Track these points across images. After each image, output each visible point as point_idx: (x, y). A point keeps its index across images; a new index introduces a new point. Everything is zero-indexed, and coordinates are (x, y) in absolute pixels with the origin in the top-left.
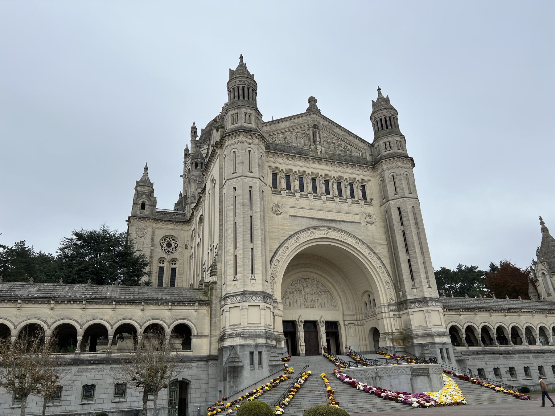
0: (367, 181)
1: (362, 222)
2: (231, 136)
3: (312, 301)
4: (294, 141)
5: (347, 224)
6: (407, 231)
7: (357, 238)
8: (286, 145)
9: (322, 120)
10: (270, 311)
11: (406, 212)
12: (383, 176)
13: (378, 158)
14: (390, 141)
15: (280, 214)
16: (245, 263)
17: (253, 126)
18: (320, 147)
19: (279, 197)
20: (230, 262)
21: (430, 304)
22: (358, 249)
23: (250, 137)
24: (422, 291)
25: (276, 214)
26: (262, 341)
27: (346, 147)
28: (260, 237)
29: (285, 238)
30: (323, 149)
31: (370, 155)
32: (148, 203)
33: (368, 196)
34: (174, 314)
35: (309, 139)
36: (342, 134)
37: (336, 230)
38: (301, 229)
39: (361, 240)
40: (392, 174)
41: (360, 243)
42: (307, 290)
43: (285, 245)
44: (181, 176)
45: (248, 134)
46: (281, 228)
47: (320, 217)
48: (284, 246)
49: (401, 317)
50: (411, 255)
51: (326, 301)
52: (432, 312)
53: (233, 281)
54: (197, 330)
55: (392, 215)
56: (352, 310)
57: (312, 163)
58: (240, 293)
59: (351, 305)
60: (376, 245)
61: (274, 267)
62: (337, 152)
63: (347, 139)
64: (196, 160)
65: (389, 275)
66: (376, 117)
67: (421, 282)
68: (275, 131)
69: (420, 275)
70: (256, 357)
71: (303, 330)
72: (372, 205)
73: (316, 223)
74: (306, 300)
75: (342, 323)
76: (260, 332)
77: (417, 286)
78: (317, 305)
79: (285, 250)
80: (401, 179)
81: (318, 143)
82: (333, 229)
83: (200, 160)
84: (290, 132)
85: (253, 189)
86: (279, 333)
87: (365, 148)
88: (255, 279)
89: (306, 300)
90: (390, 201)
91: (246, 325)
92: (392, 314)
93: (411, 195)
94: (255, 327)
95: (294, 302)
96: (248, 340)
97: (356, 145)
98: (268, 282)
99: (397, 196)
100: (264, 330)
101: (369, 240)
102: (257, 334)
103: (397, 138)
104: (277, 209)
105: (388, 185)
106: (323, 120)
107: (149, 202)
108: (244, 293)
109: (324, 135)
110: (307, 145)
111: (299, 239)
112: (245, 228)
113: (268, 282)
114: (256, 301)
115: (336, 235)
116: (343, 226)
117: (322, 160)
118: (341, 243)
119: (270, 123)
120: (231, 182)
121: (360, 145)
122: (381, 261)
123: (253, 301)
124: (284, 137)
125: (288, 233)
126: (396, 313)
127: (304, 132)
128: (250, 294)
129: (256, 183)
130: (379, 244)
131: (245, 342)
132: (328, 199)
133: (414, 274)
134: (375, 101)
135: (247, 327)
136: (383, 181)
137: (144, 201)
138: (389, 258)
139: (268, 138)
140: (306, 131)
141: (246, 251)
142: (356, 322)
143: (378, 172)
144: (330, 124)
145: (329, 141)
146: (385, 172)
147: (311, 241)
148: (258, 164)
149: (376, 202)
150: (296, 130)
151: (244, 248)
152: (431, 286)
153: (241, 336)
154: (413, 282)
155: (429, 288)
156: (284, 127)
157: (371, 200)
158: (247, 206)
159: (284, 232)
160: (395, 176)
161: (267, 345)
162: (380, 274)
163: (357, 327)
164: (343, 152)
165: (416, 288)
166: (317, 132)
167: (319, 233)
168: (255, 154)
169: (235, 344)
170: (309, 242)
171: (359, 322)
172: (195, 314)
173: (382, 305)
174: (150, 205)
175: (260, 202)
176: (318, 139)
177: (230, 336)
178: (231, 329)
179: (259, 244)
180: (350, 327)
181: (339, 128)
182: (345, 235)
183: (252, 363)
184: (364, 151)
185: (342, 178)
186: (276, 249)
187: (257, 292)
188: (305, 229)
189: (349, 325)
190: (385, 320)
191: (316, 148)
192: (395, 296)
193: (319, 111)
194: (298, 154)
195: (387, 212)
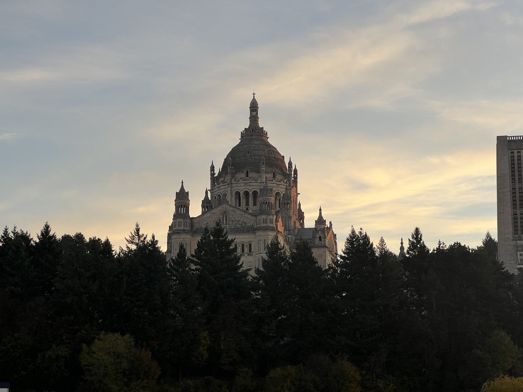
0: (252, 242)
17: (182, 228)
23: (179, 235)
30: (228, 226)
36: (241, 214)
45: (178, 234)
63: (244, 217)
72: (252, 256)
80: (261, 243)
83: (205, 204)
99: (259, 252)
127: (218, 217)
140: (220, 216)
150: (214, 217)
157: (253, 252)
164: (240, 225)
176: (225, 221)
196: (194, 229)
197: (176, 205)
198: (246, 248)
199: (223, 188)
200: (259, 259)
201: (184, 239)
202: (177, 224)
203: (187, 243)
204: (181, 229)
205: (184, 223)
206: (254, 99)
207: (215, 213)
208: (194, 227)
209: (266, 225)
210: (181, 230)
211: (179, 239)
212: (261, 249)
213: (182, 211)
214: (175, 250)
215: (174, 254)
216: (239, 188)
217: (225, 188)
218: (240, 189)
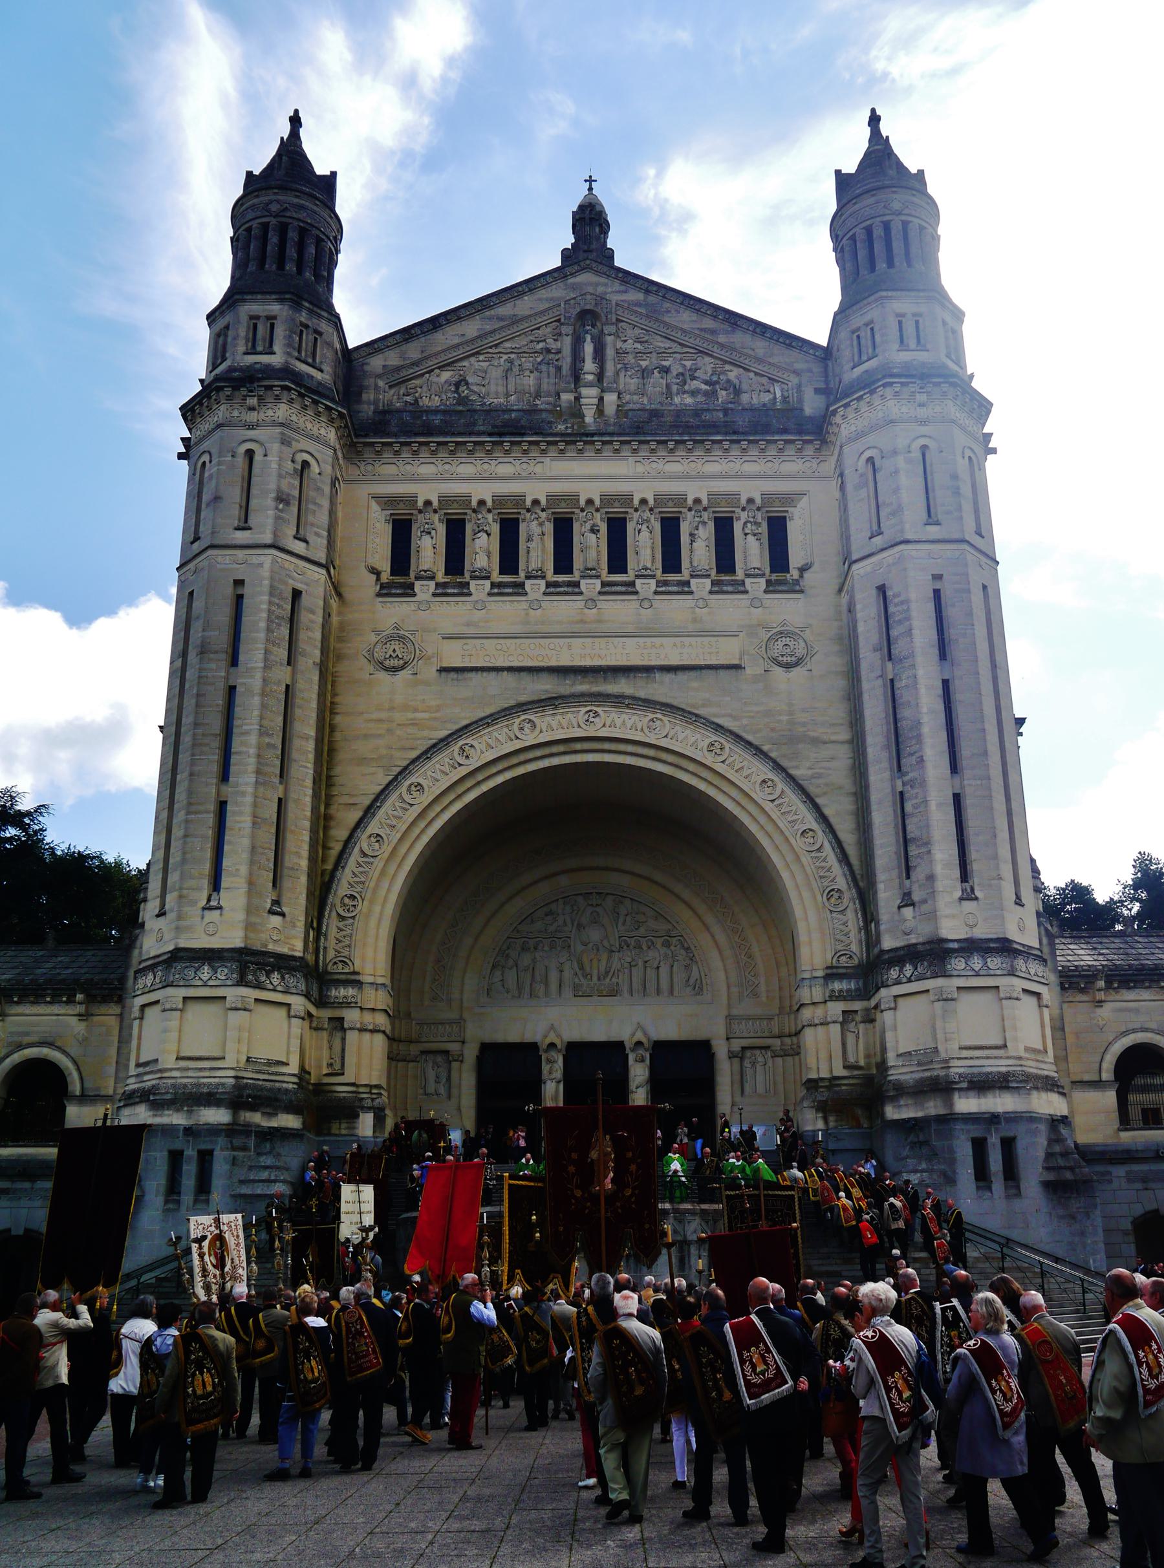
0: (790, 499)
1: (746, 662)
3: (607, 973)
4: (493, 388)
5: (682, 677)
6: (901, 680)
7: (718, 728)
8: (460, 408)
9: (617, 286)
10: (289, 1016)
11: (902, 603)
14: (872, 322)
15: (403, 668)
16: (188, 856)
18: (594, 391)
19: (405, 605)
21: (957, 964)
22: (719, 768)
23: (253, 401)
24: (933, 916)
25: (387, 669)
26: (217, 1116)
27: (715, 378)
28: (252, 760)
29: (414, 754)
31: (817, 391)
33: (795, 559)
34: (13, 1030)
35: (559, 369)
36: (701, 330)
37: (628, 706)
38: (482, 715)
39: (731, 733)
40: (867, 454)
41: (727, 746)
42: (595, 935)
43: (413, 779)
46: (398, 717)
47: (565, 661)
48: (407, 783)
49: (872, 1021)
50: (907, 773)
51: (664, 971)
52: (967, 999)
53: (158, 916)
54: (81, 1079)
56: (764, 999)
57: (554, 458)
58: (165, 957)
59: (762, 980)
60: (800, 746)
61: (360, 860)
62: (677, 400)
63: (722, 346)
65: (844, 858)
67: (931, 878)
68: (416, 364)
69: (929, 852)
70: (190, 1170)
71: (558, 1073)
72: (802, 592)
73: (546, 686)
74: (582, 968)
75: (721, 1050)
76: (218, 1085)
77: (916, 897)
78: (625, 988)
79: (407, 798)
80: (896, 472)
81: (590, 377)
84: (481, 358)
85: (247, 591)
86: (362, 1090)
87: (799, 366)
88: (220, 908)
89: (582, 968)
91: (169, 1061)
92: (836, 1009)
93: (933, 531)
94: (201, 1069)
95: (538, 978)
96: (166, 1112)
97: (760, 361)
98: (283, 915)
99: (878, 541)
100: (232, 1081)
101: (773, 730)
102: (202, 1094)
104: (390, 652)
106: (623, 288)
108: (179, 957)
109: (625, 346)
110: (549, 395)
111: (472, 750)
112: (199, 731)
113: (283, 915)
114: (211, 983)
115: (629, 724)
116: (662, 689)
117: (593, 442)
119: (398, 337)
122: (817, 808)
123: (200, 983)
124: (456, 379)
125: (426, 733)
126: (857, 1005)
127: (541, 345)
129: (261, 565)
130: (816, 742)
131: (157, 1120)
132: (607, 589)
133: (913, 850)
134: (850, 167)
135: (171, 1070)
136: (842, 488)
138: (855, 794)
139: (392, 391)
141: (196, 813)
142: (778, 1042)
144: (652, 299)
145: (644, 364)
146: (846, 449)
147: (522, 757)
148: (273, 495)
149: (820, 580)
150: (508, 345)
151: (190, 804)
152: (978, 893)
153: (148, 1100)
154: (907, 882)
155: (966, 903)
156: (456, 341)
157: (802, 570)
158: (216, 652)
159: (411, 730)
161: (232, 1131)
162: (805, 859)
163: (779, 1060)
164: (700, 398)
165: (913, 904)
166: (588, 338)
167: (554, 724)
168: (323, 463)
170: (515, 760)
171: (788, 1040)
172: (78, 1027)
173: (807, 975)
175: (269, 630)
176: (589, 365)
178: (137, 1076)
179: (247, 784)
180: (754, 1064)
181: (688, 307)
182: (666, 719)
183: (173, 1189)
185: (681, 500)
186: (373, 797)
187: (221, 951)
188: (499, 712)
189: (748, 1053)
191: (577, 399)
192: (860, 941)
193: (610, 255)
194: (490, 435)
196: (367, 410)
198: (750, 538)
200: (882, 590)
201: (287, 432)
202: (242, 332)
203: (305, 464)
204: (269, 365)
205: (292, 332)
207: (515, 320)
208: (365, 397)
209: (922, 356)
210: (268, 372)
211: (251, 427)
212: (898, 511)
214: (208, 505)
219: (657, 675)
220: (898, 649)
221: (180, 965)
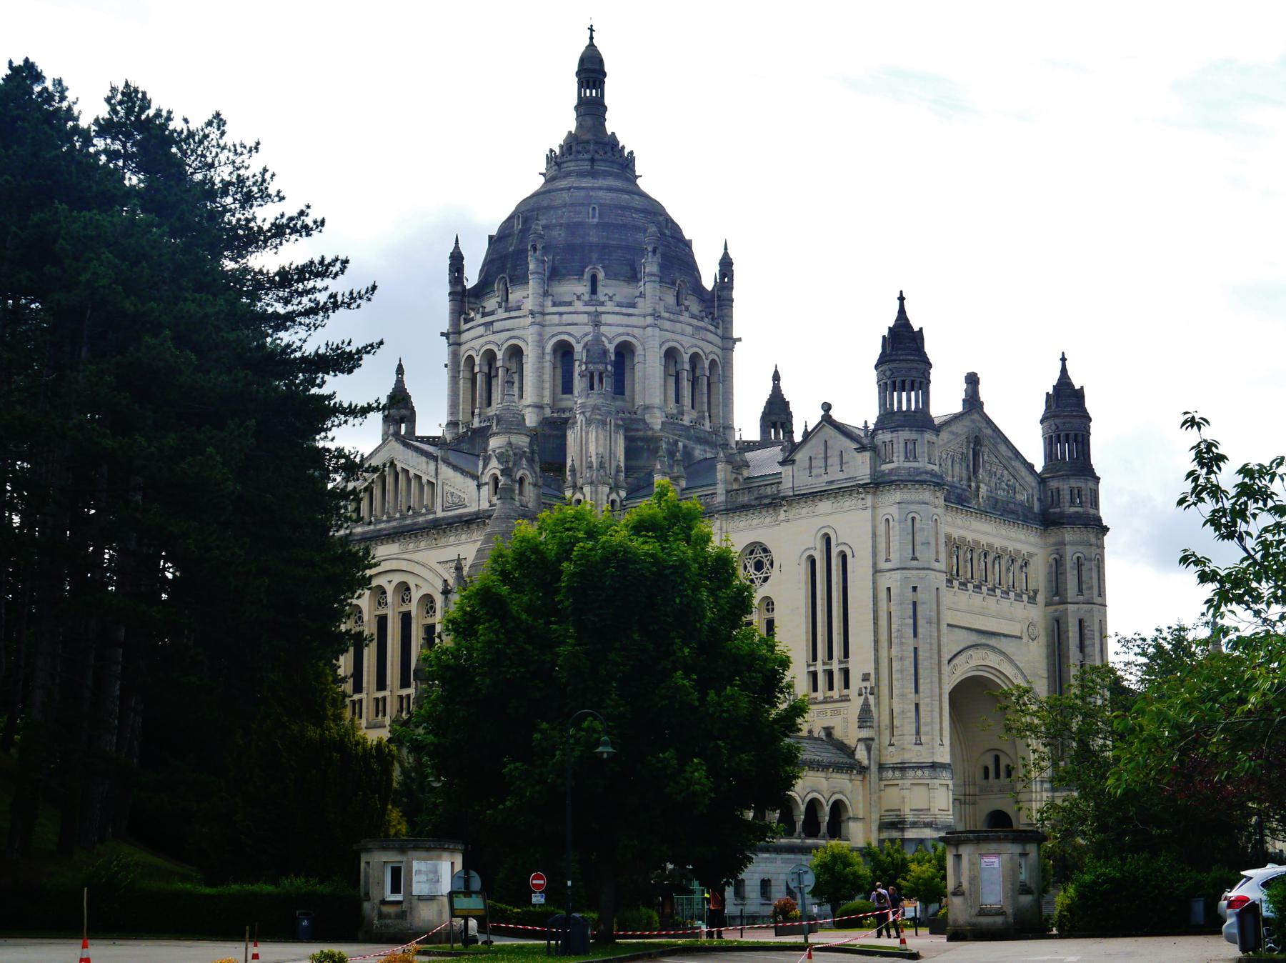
1: (1024, 637)
2: (909, 486)
7: (1017, 667)
12: (1060, 552)
13: (1055, 513)
20: (909, 714)
32: (531, 481)
40: (1079, 555)
44: (442, 334)
55: (1068, 631)
64: (601, 367)
66: (1060, 428)
73: (974, 638)
80: (1091, 569)
82: (993, 648)
90: (1069, 606)
91: (937, 812)
92: (1045, 795)
99: (1081, 598)
103: (1091, 484)
105: (1068, 575)
107: (532, 477)
118: (997, 674)
120: (908, 575)
121: (1027, 479)
128: (940, 767)
137: (525, 474)
143: (1052, 540)
160: (1082, 560)
169: (923, 837)
171: (967, 797)
172: (848, 785)
174: (535, 485)
177: (914, 825)
178: (914, 815)
184: (1031, 491)
190: (1034, 803)
191: (978, 488)
194: (962, 505)
195: (1058, 622)
197: (881, 383)
199: (619, 323)
206: (591, 46)
212: (1091, 588)
213: (906, 401)
215: (888, 560)
216: (678, 337)
217: (630, 323)
218: (684, 345)
219: (1002, 638)
220: (1088, 650)
221: (938, 770)
